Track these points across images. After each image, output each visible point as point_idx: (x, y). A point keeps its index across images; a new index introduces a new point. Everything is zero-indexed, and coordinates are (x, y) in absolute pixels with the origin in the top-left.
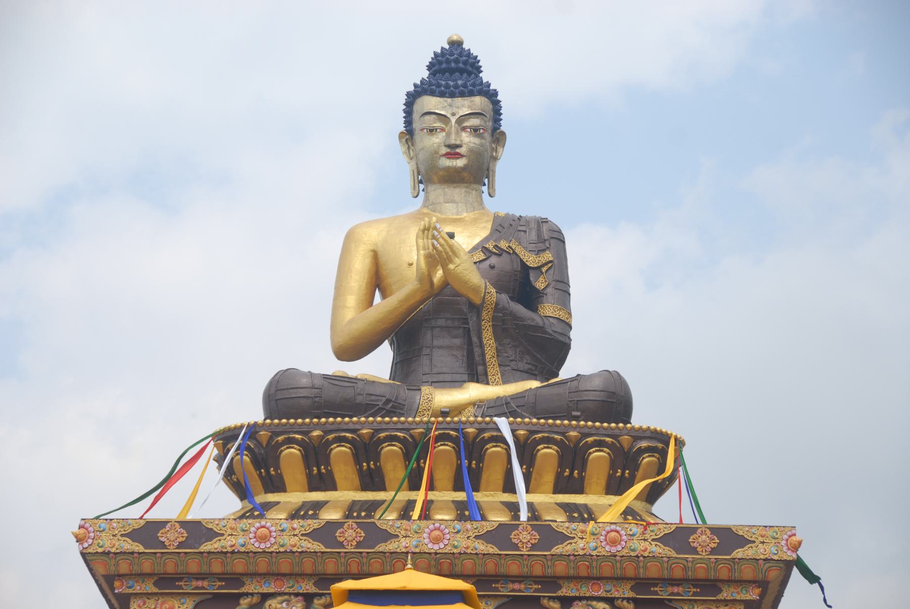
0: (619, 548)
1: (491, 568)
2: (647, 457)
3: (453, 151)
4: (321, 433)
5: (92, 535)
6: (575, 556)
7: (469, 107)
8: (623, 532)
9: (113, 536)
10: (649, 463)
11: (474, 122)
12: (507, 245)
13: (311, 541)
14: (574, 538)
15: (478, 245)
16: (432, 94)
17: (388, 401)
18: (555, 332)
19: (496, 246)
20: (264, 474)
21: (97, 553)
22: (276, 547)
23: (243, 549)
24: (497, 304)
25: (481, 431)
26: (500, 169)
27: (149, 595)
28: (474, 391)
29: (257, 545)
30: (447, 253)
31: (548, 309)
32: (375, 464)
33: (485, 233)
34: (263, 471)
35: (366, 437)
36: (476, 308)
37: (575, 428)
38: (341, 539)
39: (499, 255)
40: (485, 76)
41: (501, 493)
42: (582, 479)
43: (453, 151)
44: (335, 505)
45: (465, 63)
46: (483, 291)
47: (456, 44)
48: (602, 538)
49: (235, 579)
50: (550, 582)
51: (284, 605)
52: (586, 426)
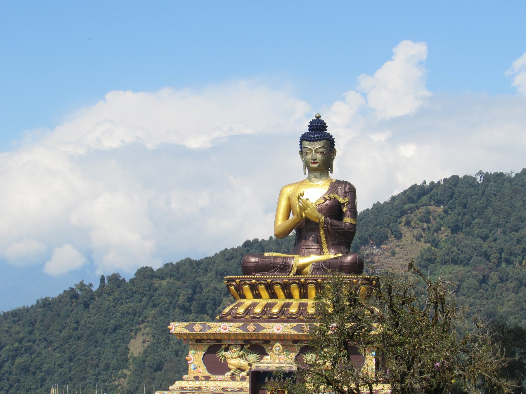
1: (296, 338)
5: (174, 327)
7: (319, 145)
15: (322, 196)
16: (307, 140)
18: (348, 229)
22: (229, 332)
23: (219, 332)
25: (306, 280)
26: (335, 163)
27: (194, 345)
29: (223, 331)
31: (347, 220)
32: (273, 291)
33: (326, 190)
35: (269, 283)
36: (317, 224)
38: (249, 329)
39: (330, 200)
43: (314, 161)
45: (320, 126)
47: (318, 118)
49: (220, 341)
51: (235, 348)
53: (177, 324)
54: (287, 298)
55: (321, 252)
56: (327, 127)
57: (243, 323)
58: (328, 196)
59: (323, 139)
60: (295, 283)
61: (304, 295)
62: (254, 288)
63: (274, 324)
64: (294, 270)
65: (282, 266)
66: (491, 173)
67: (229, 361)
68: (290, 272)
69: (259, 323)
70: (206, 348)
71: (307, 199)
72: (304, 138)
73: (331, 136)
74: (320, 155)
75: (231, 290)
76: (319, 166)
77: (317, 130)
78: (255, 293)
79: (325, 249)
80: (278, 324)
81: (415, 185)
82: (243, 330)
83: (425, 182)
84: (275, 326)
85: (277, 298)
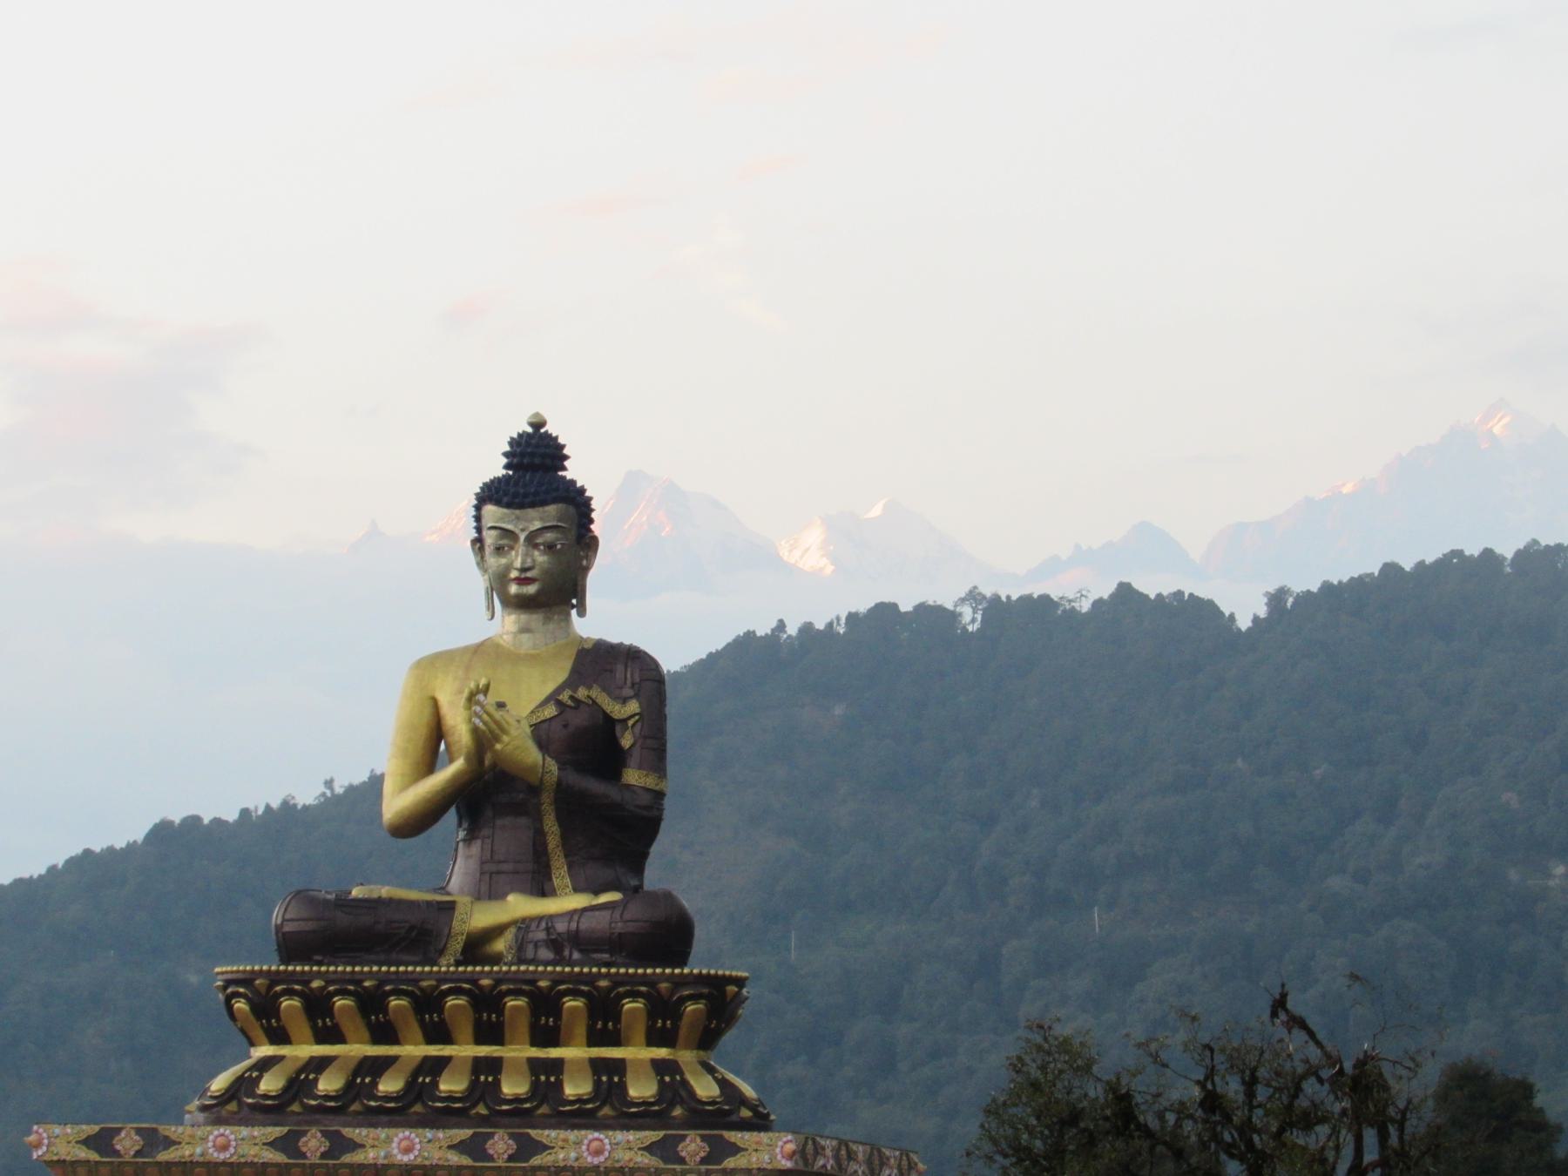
0: (602, 1159)
2: (690, 1005)
4: (323, 983)
6: (555, 1167)
7: (541, 519)
8: (607, 1141)
9: (69, 1142)
10: (694, 1010)
11: (549, 536)
12: (586, 693)
13: (273, 1150)
14: (553, 1148)
17: (412, 928)
18: (638, 806)
19: (572, 697)
20: (266, 1025)
21: (52, 1161)
22: (235, 1158)
23: (201, 1159)
24: (559, 783)
28: (519, 906)
29: (215, 1154)
30: (491, 732)
31: (633, 776)
33: (561, 676)
34: (264, 1021)
36: (535, 790)
37: (608, 975)
38: (304, 1149)
41: (528, 1047)
42: (617, 1032)
44: (347, 1058)
46: (541, 770)
47: (538, 424)
48: (584, 1147)
52: (617, 973)
53: (57, 1130)
54: (430, 1040)
55: (542, 888)
56: (566, 457)
57: (285, 1129)
58: (570, 693)
59: (555, 501)
63: (392, 1131)
64: (457, 945)
65: (414, 934)
66: (1008, 597)
68: (441, 952)
69: (341, 1129)
71: (501, 705)
72: (492, 493)
73: (582, 491)
74: (544, 553)
75: (236, 1014)
76: (539, 593)
77: (532, 468)
78: (320, 1024)
79: (561, 875)
80: (407, 1133)
81: (750, 635)
82: (284, 1150)
83: (781, 626)
84: (396, 1139)
85: (394, 1040)
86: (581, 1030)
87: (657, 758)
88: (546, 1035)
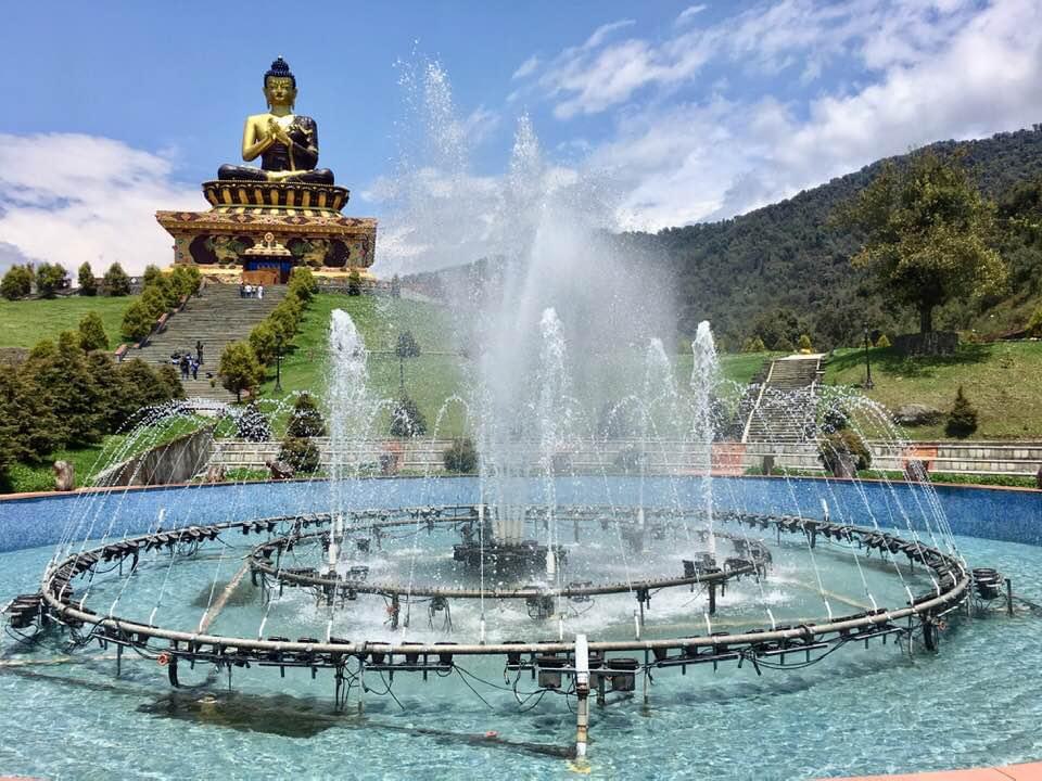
1: (286, 229)
3: (279, 95)
28: (285, 173)
31: (311, 148)
36: (286, 148)
40: (291, 71)
49: (208, 231)
50: (305, 234)
60: (274, 188)
61: (282, 201)
62: (234, 192)
67: (218, 252)
70: (192, 239)
85: (256, 203)
86: (308, 202)
87: (316, 146)
88: (298, 203)
